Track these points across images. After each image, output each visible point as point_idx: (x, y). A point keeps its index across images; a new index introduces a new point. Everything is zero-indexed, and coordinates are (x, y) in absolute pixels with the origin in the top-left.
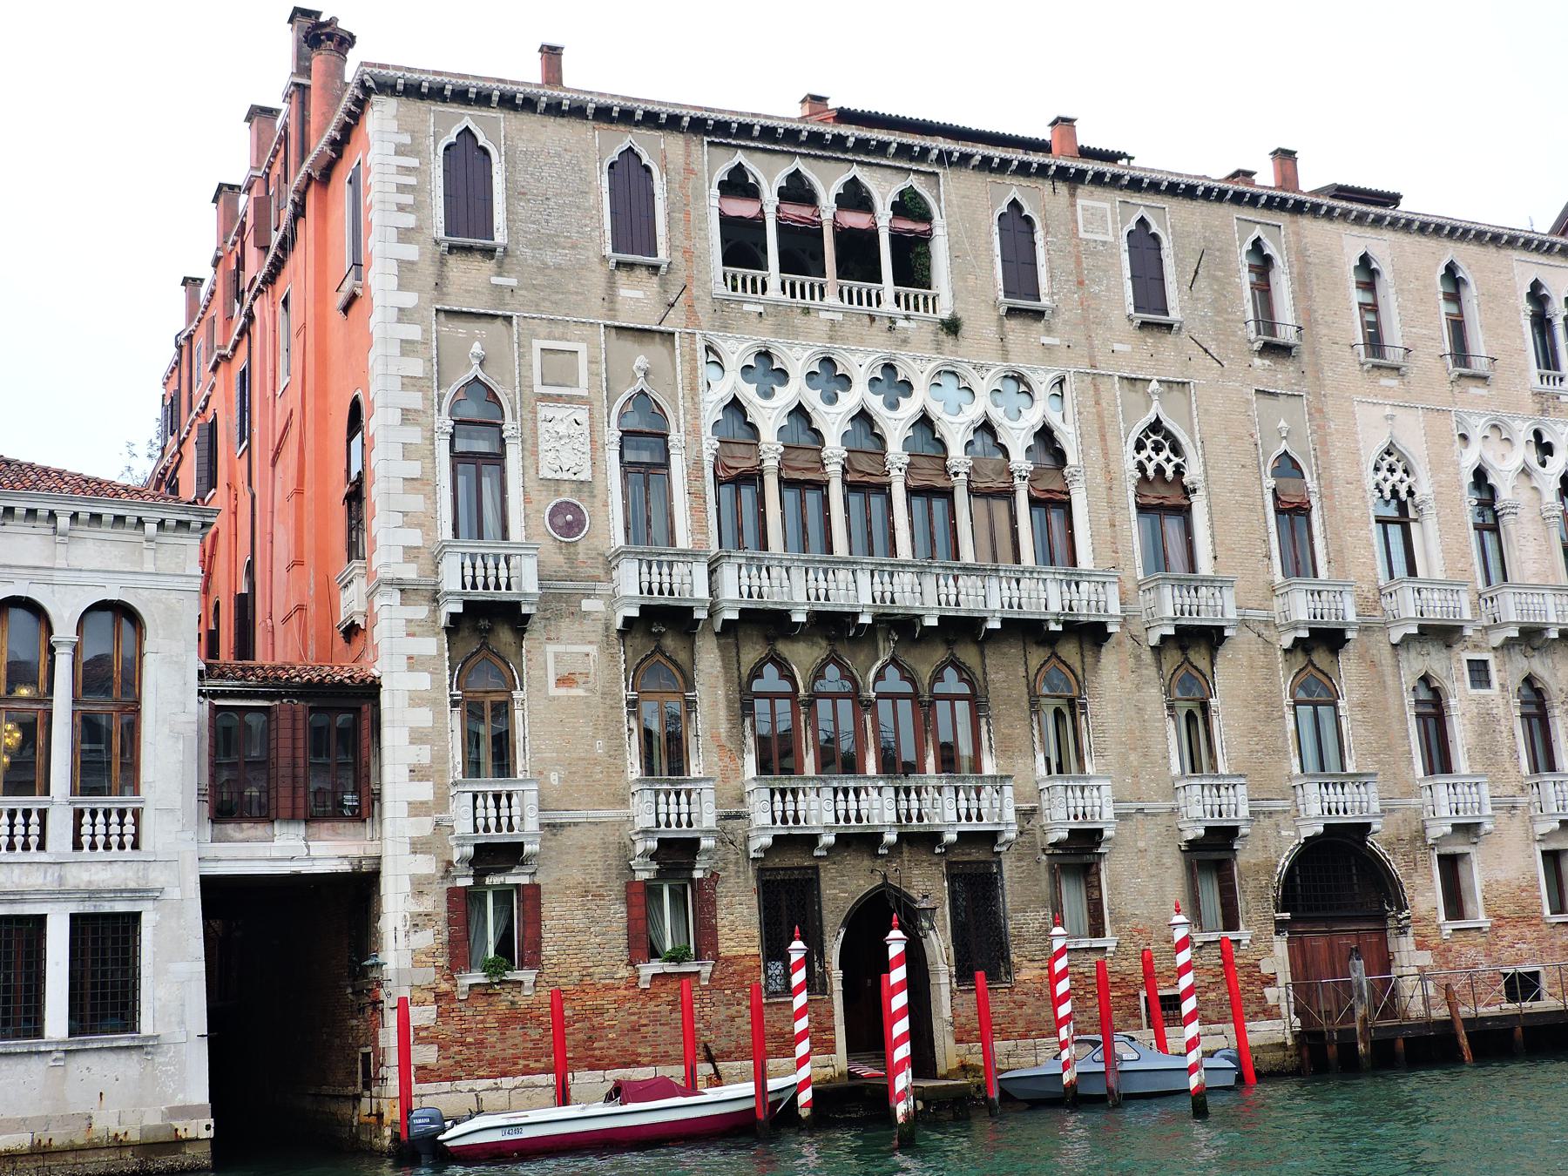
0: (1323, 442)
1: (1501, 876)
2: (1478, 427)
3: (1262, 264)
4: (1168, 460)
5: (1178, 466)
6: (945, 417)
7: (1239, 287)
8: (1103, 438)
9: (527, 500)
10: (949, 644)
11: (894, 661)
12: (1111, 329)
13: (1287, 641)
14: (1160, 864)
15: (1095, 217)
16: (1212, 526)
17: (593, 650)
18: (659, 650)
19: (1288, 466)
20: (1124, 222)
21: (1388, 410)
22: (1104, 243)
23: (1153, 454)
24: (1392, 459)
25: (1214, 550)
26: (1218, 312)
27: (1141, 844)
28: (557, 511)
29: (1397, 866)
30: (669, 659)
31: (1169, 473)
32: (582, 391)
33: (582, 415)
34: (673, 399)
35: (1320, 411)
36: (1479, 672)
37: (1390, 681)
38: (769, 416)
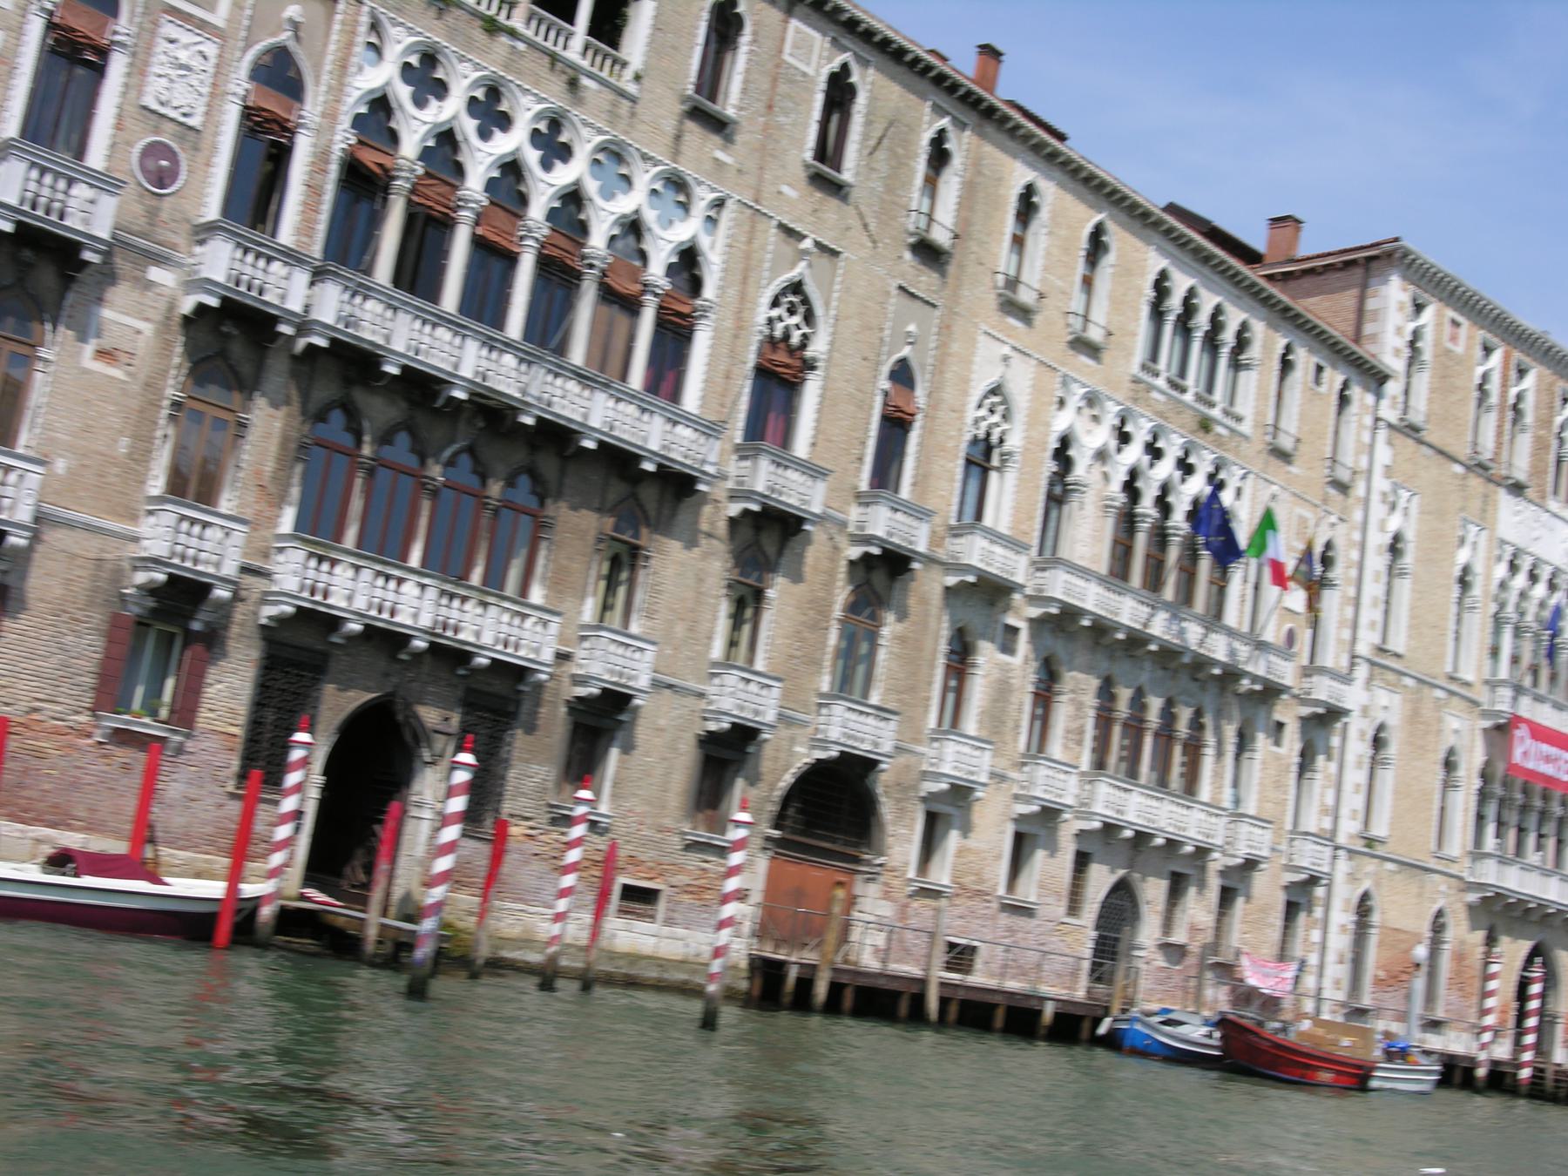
3: (939, 156)
4: (798, 327)
5: (805, 336)
6: (599, 201)
7: (913, 171)
8: (745, 280)
9: (119, 126)
10: (534, 448)
11: (471, 450)
12: (783, 167)
13: (855, 552)
16: (819, 411)
17: (147, 328)
18: (223, 354)
19: (903, 374)
20: (830, 60)
21: (1006, 350)
22: (805, 74)
23: (785, 314)
24: (996, 399)
25: (815, 436)
26: (890, 190)
27: (662, 722)
28: (153, 150)
30: (231, 367)
31: (795, 339)
32: (219, 18)
33: (211, 49)
34: (317, 67)
35: (948, 327)
38: (414, 129)
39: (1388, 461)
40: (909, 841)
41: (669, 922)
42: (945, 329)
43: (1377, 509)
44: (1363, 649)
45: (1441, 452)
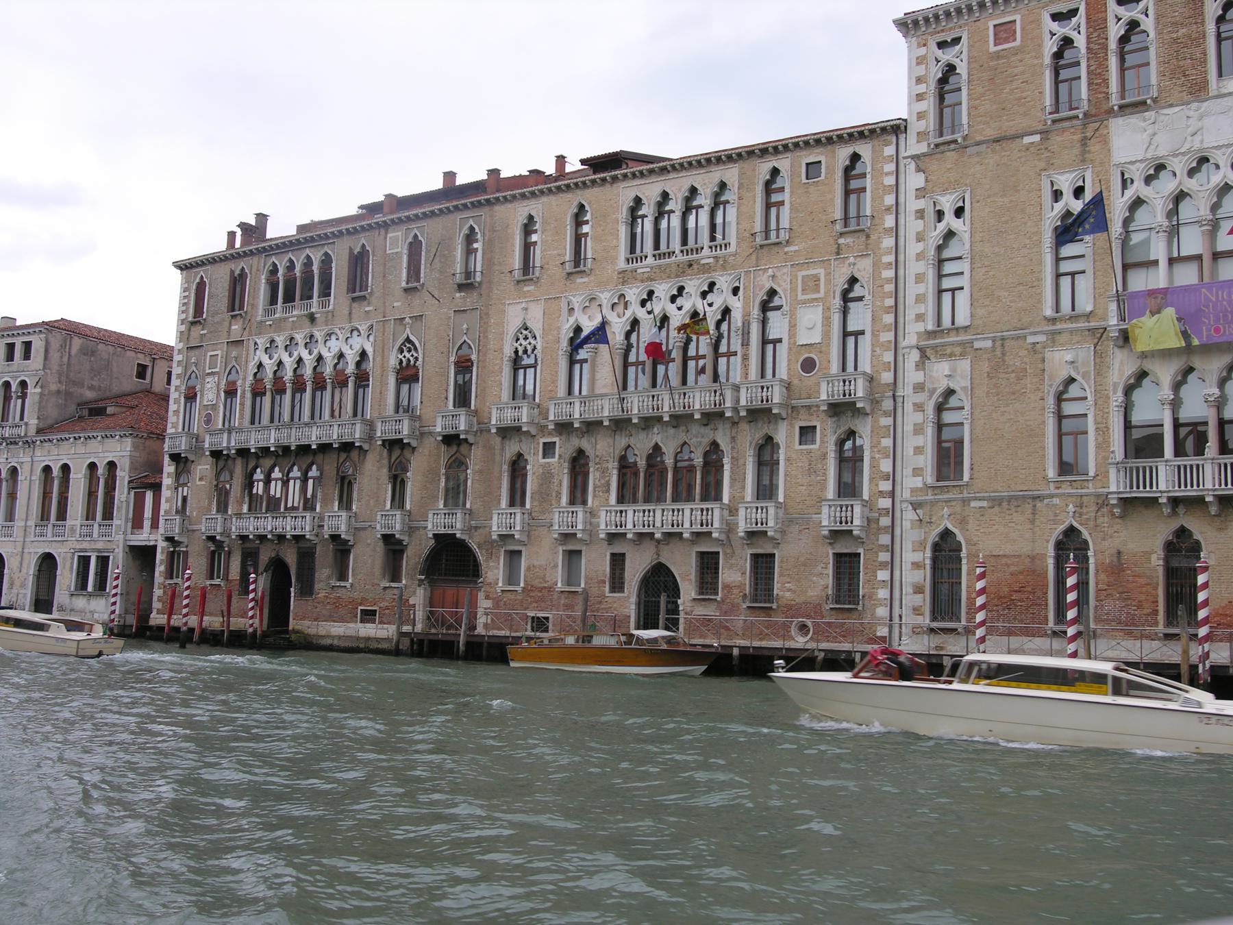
0: (484, 331)
1: (536, 563)
2: (577, 302)
14: (374, 551)
15: (397, 238)
29: (481, 558)
35: (487, 314)
36: (548, 449)
37: (498, 458)
39: (921, 184)
40: (498, 568)
41: (380, 623)
42: (484, 316)
43: (912, 226)
44: (911, 337)
45: (997, 141)
